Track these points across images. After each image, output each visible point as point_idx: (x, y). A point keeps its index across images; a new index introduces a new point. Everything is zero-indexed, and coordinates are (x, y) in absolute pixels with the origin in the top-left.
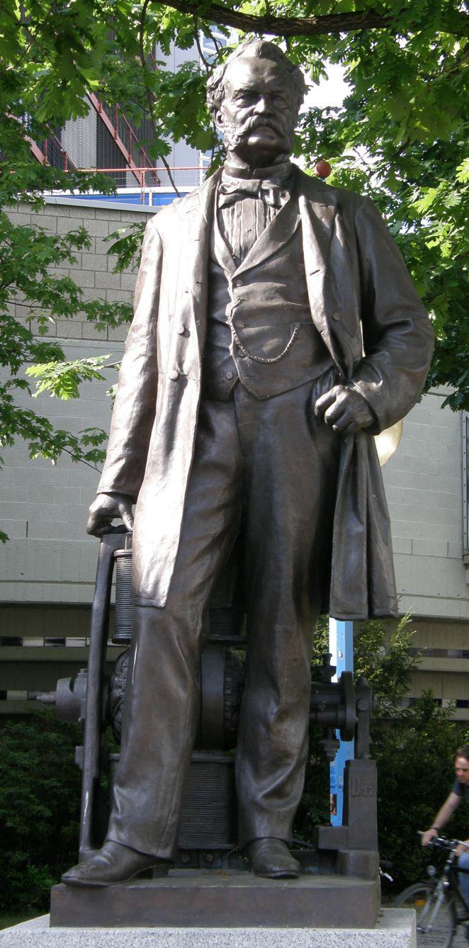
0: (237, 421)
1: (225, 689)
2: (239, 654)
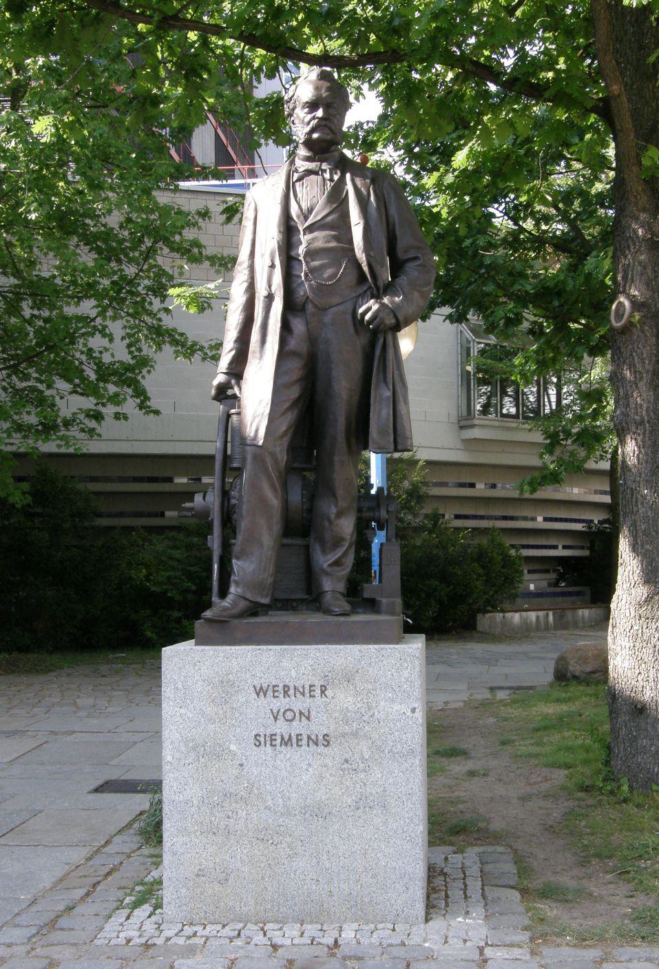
0: (307, 324)
1: (302, 498)
2: (311, 476)
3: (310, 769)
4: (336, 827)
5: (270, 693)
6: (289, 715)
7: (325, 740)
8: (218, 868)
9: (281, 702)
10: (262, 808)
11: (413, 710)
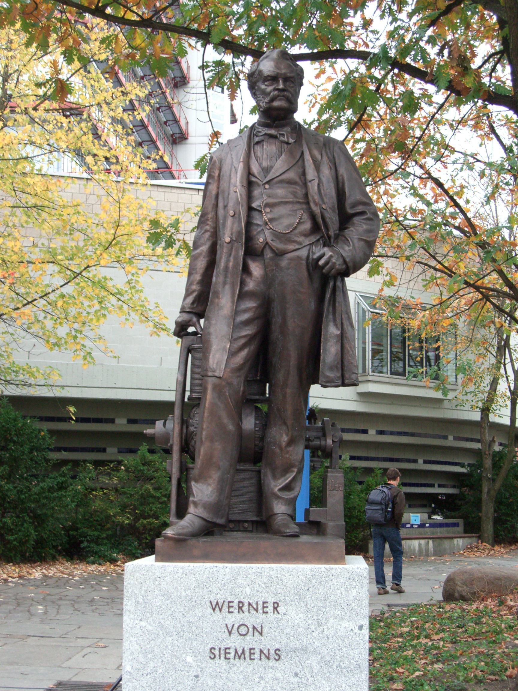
0: (265, 267)
1: (255, 427)
2: (264, 408)
3: (262, 682)
5: (225, 609)
6: (243, 630)
9: (235, 617)
11: (361, 628)
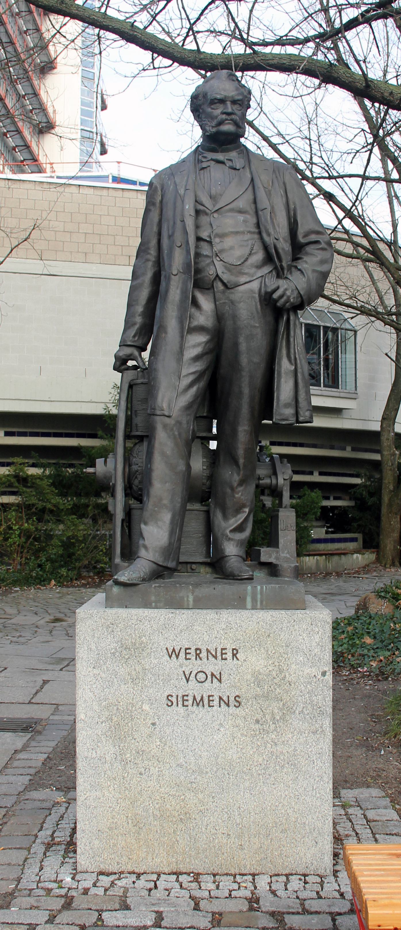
3: (222, 729)
4: (247, 784)
5: (182, 655)
6: (202, 677)
7: (237, 701)
8: (130, 822)
9: (193, 664)
10: (174, 766)
11: (324, 674)
